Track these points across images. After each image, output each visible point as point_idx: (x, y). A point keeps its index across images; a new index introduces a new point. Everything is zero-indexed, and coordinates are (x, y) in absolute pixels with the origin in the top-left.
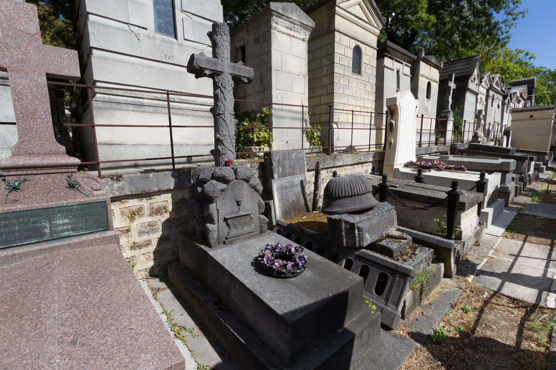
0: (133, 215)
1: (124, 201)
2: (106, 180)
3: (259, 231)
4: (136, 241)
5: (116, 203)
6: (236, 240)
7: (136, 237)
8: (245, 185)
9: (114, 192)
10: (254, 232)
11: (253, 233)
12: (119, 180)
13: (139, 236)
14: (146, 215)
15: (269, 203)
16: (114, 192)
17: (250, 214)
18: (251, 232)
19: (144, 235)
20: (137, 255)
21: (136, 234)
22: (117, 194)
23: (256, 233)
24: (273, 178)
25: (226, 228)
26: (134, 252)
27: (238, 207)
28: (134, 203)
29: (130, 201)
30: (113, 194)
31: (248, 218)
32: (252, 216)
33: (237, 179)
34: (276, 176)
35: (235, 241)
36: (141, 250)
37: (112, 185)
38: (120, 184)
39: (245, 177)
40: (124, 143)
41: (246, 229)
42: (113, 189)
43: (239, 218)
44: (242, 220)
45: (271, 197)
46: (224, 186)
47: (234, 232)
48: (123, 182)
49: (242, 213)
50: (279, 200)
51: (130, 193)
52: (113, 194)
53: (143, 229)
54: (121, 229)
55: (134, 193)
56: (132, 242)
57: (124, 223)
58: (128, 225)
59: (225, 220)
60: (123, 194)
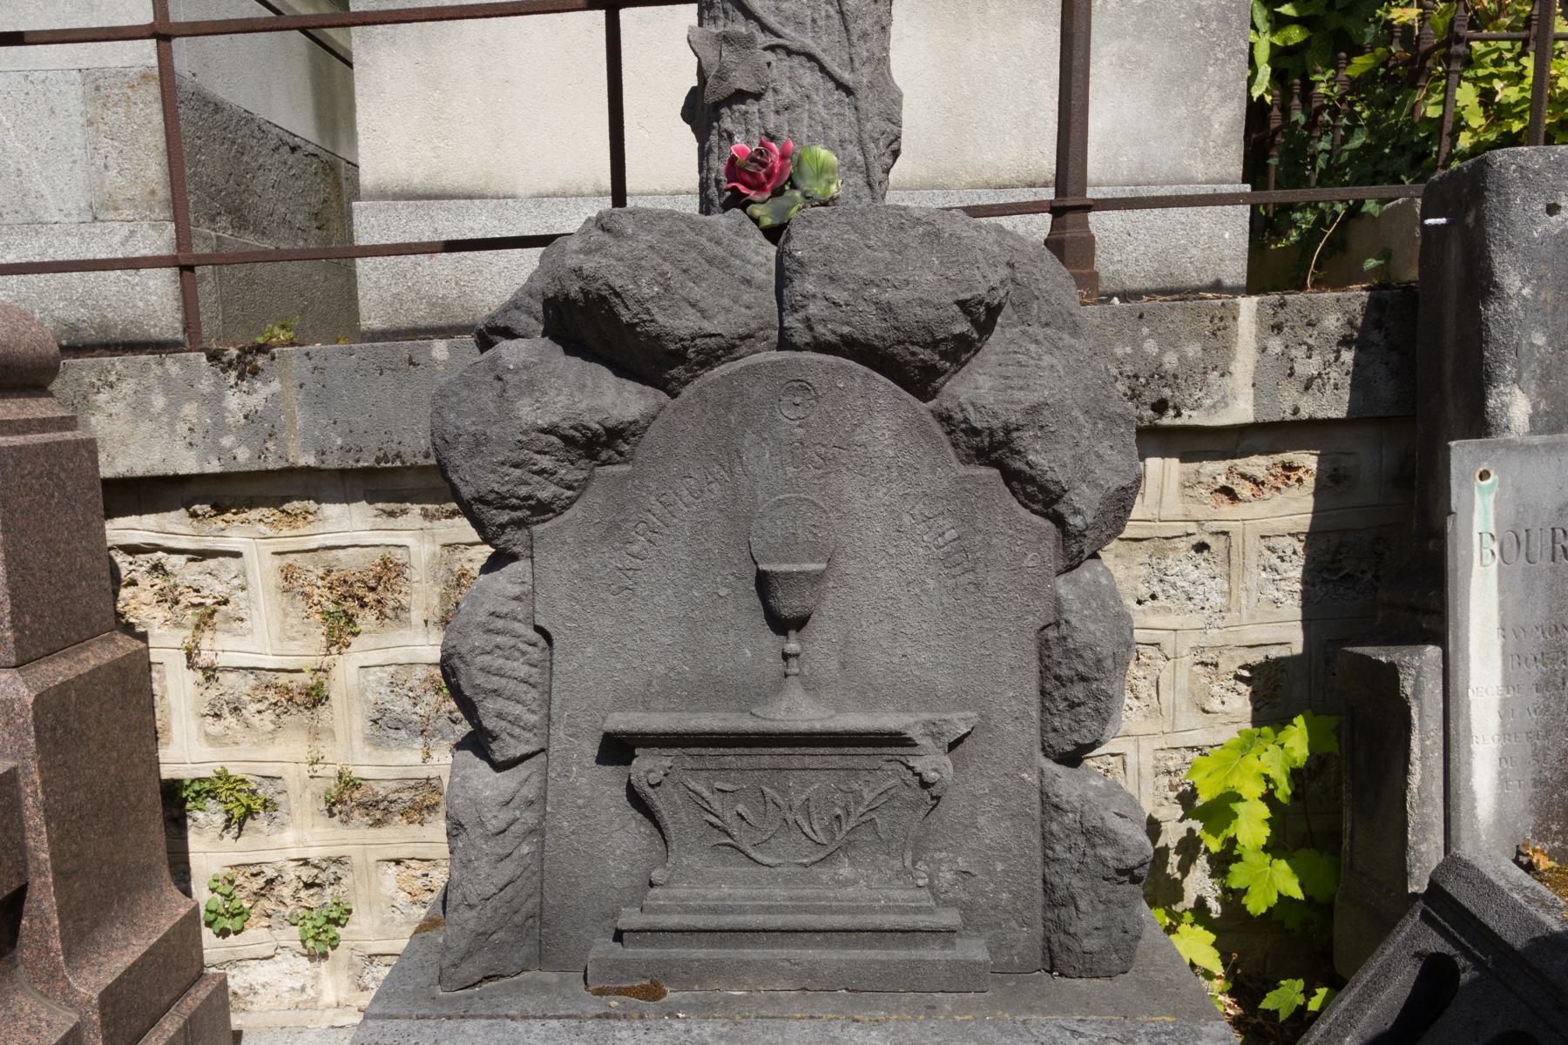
0: (352, 602)
1: (294, 506)
2: (186, 365)
3: (1026, 937)
4: (358, 773)
5: (254, 514)
6: (715, 969)
7: (358, 744)
8: (881, 413)
9: (227, 441)
10: (946, 934)
11: (934, 953)
12: (255, 372)
13: (375, 742)
14: (416, 616)
15: (1391, 673)
16: (227, 441)
17: (897, 739)
18: (908, 934)
19: (401, 745)
20: (356, 859)
21: (359, 724)
22: (244, 458)
23: (975, 950)
24: (1479, 424)
25: (630, 833)
26: (342, 832)
27: (769, 639)
28: (349, 526)
29: (332, 510)
30: (221, 452)
31: (886, 774)
32: (932, 762)
33: (785, 342)
34: (1515, 406)
35: (690, 975)
36: (385, 833)
37: (214, 402)
38: (260, 394)
39: (872, 327)
40: (494, 187)
41: (861, 887)
42: (220, 427)
43: (766, 757)
44: (813, 780)
45: (1426, 612)
46: (617, 399)
47: (703, 886)
48: (276, 386)
49: (800, 712)
50: (1513, 657)
51: (309, 460)
52: (221, 452)
53: (401, 706)
54: (283, 679)
55: (333, 462)
56: (331, 771)
57: (294, 647)
58: (313, 662)
59: (617, 749)
60: (272, 464)
